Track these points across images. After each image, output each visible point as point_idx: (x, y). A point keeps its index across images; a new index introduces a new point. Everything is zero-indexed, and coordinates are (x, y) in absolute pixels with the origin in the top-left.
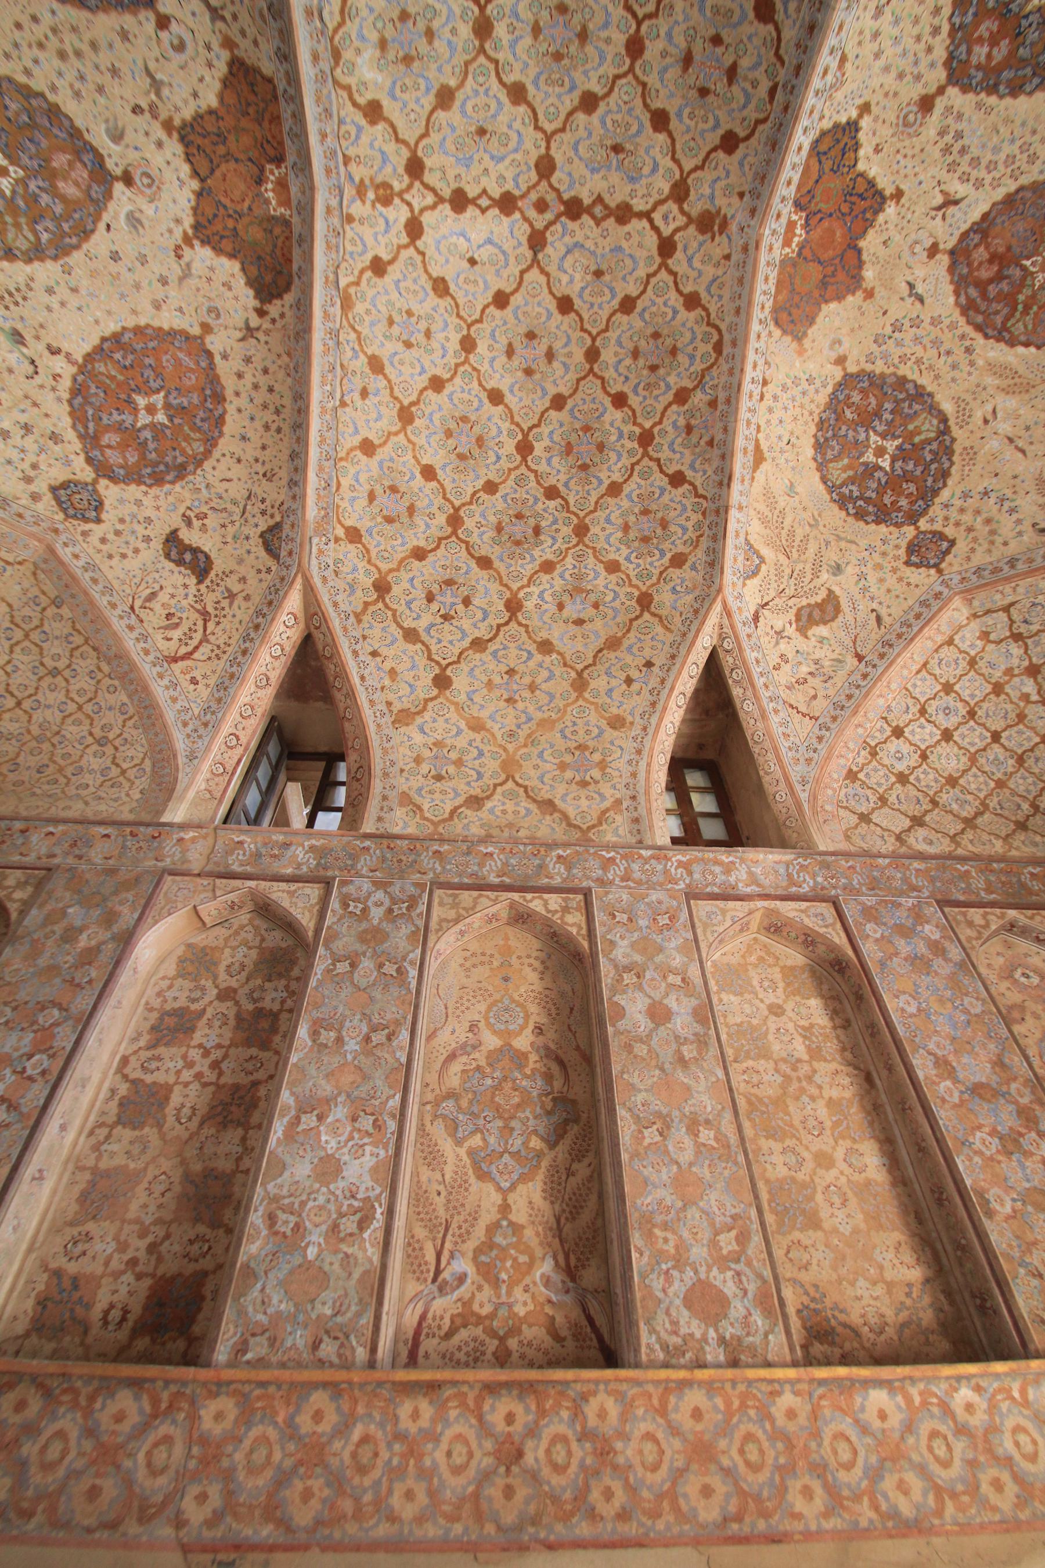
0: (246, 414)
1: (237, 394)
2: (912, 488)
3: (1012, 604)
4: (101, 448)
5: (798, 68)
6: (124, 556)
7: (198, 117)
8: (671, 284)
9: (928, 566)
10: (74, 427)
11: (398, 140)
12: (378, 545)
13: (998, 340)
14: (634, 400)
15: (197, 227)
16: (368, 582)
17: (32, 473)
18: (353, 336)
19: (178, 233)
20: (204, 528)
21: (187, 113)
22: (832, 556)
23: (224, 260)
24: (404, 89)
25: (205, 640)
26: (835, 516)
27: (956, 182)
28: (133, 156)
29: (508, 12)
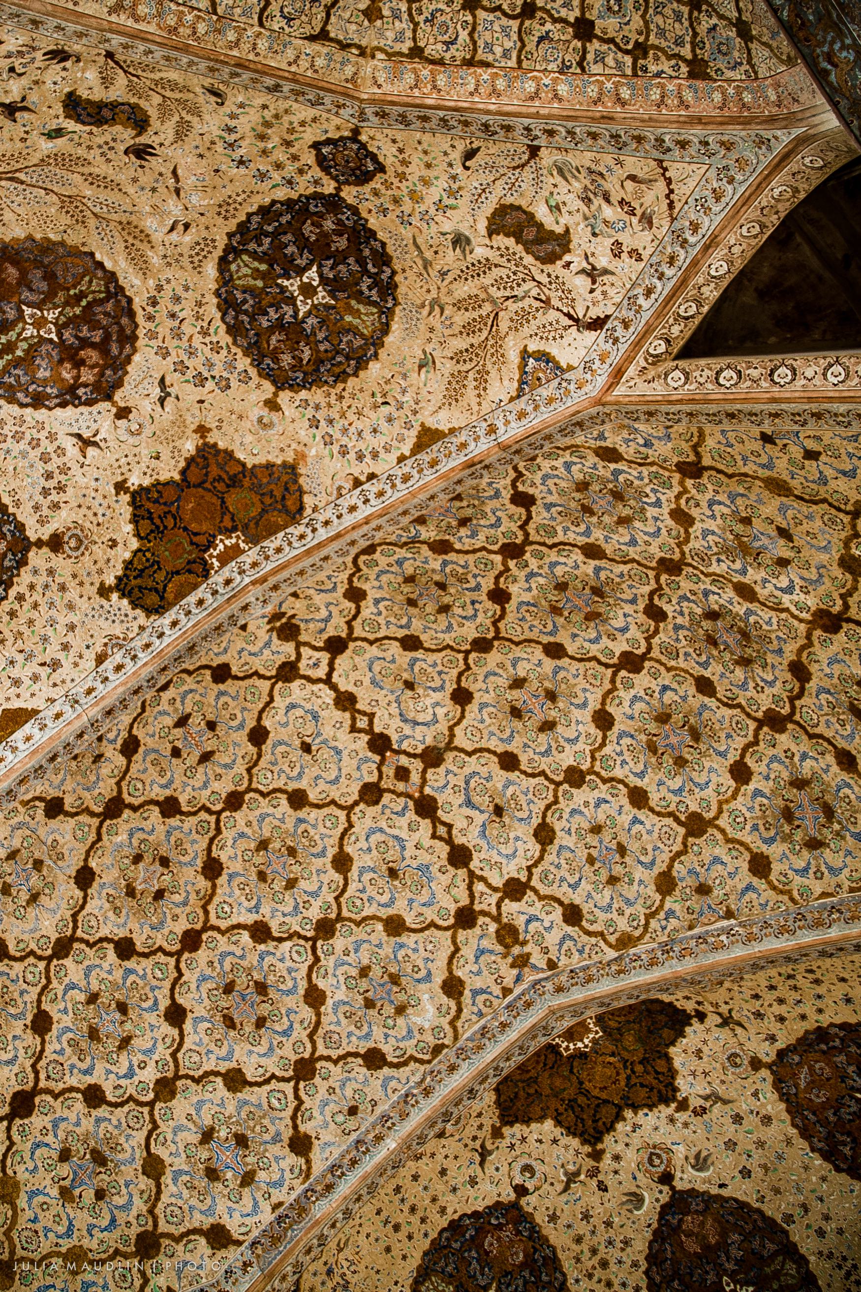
2: (308, 229)
3: (312, 38)
5: (136, 692)
8: (359, 620)
9: (363, 146)
11: (457, 950)
13: (122, 289)
14: (487, 584)
21: (575, 1142)
22: (450, 258)
24: (416, 969)
26: (410, 288)
27: (68, 454)
29: (300, 916)
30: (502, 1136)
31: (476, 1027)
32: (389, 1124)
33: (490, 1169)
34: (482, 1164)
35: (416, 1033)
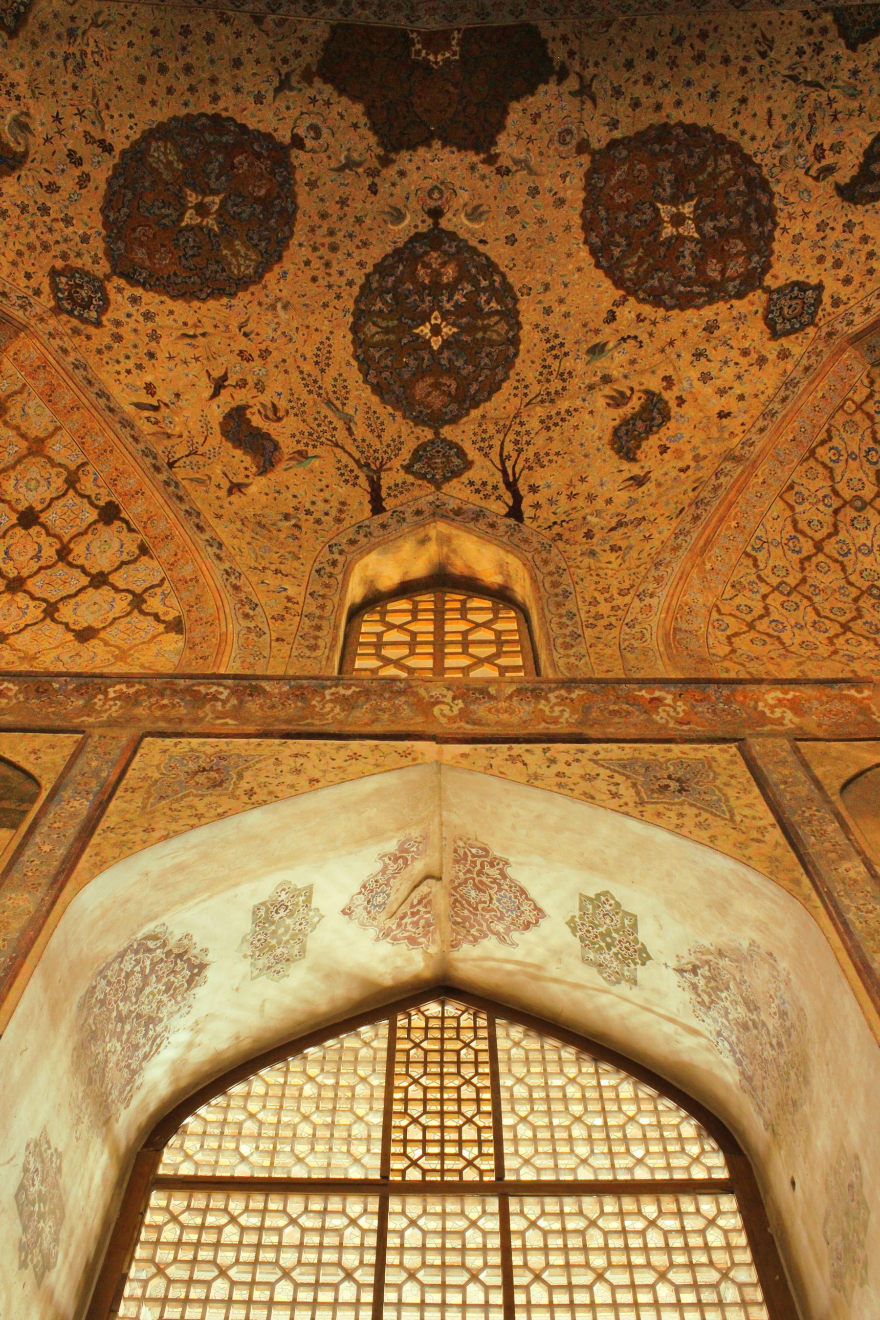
4: (725, 280)
7: (374, 128)
10: (699, 308)
17: (754, 356)
20: (837, 148)
21: (373, 140)
23: (510, 120)
28: (413, 203)
30: (310, 83)
33: (281, 104)
34: (277, 91)
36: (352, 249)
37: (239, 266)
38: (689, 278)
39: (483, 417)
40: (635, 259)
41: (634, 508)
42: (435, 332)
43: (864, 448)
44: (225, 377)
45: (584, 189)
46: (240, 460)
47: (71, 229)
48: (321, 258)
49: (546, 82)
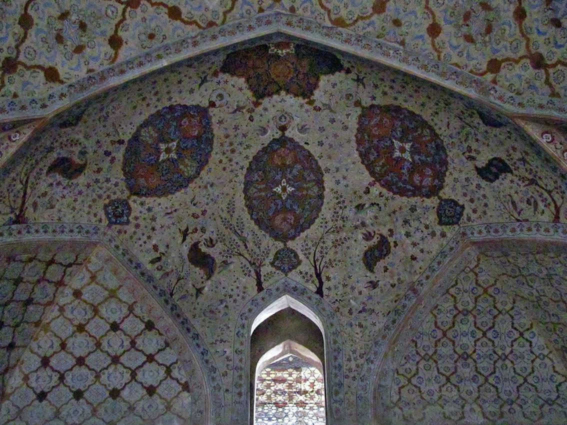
0: (408, 98)
1: (396, 99)
6: (486, 205)
7: (251, 88)
12: (505, 47)
15: (304, 96)
16: (530, 72)
17: (430, 230)
18: (360, 23)
19: (307, 107)
20: (478, 152)
21: (249, 94)
25: (549, 192)
28: (272, 124)
31: (237, 22)
32: (168, 52)
34: (200, 85)
35: (203, 8)
36: (241, 150)
37: (188, 171)
38: (405, 180)
39: (307, 237)
40: (381, 164)
41: (370, 301)
42: (284, 189)
43: (471, 287)
44: (187, 229)
45: (358, 123)
46: (198, 272)
47: (110, 183)
48: (227, 157)
49: (340, 71)
